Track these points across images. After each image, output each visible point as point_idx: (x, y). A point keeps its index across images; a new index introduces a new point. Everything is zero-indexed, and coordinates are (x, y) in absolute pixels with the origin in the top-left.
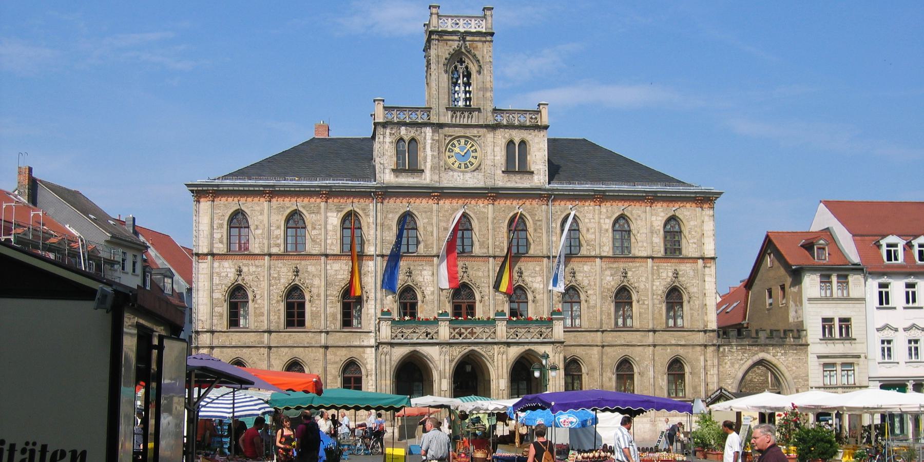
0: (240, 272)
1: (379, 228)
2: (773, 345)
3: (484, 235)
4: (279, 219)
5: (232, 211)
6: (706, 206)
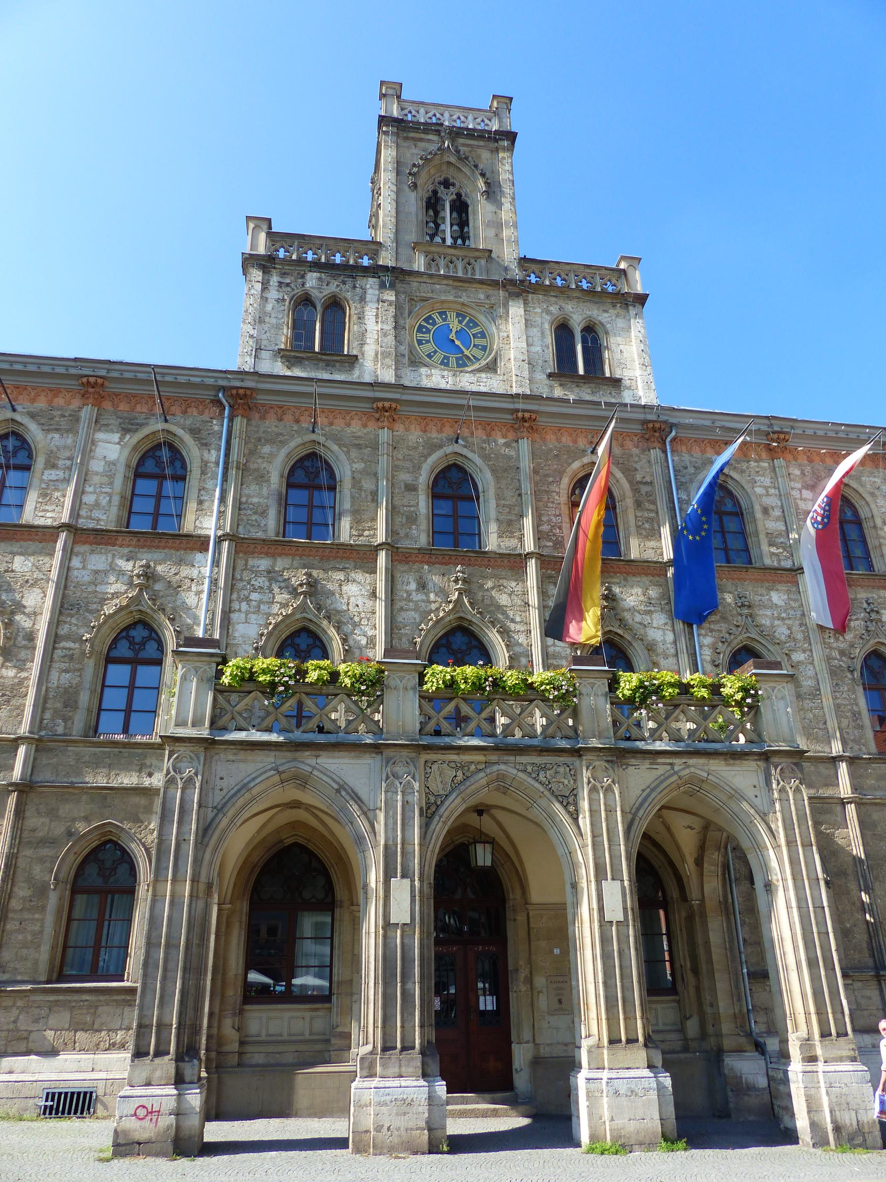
1: (233, 472)
3: (510, 507)
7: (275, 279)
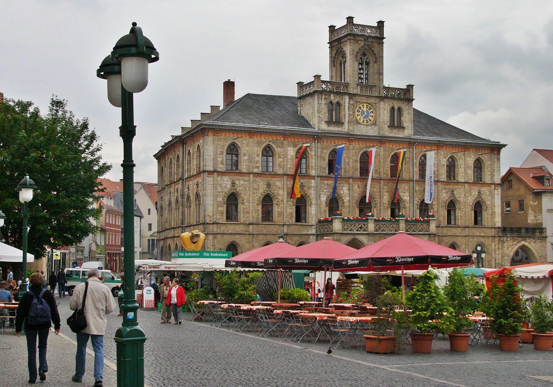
0: (233, 184)
2: (529, 237)
4: (259, 150)
5: (229, 143)
7: (323, 96)
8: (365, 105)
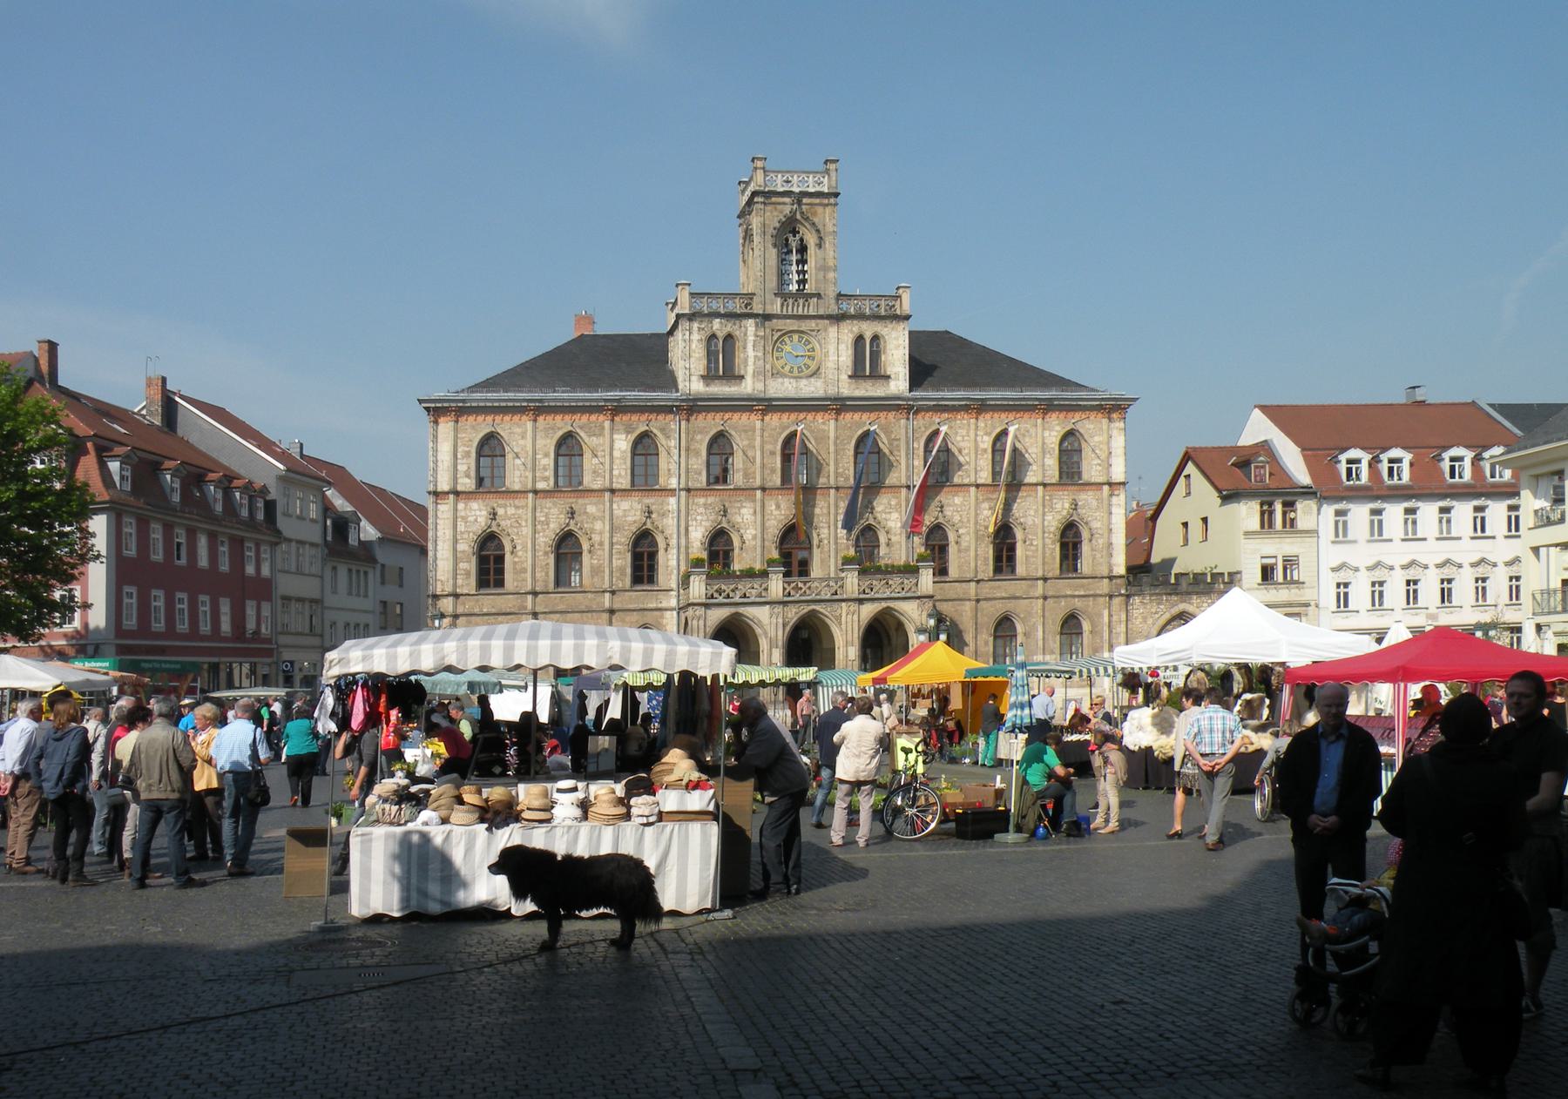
4: (548, 444)
6: (1114, 416)
8: (796, 337)
